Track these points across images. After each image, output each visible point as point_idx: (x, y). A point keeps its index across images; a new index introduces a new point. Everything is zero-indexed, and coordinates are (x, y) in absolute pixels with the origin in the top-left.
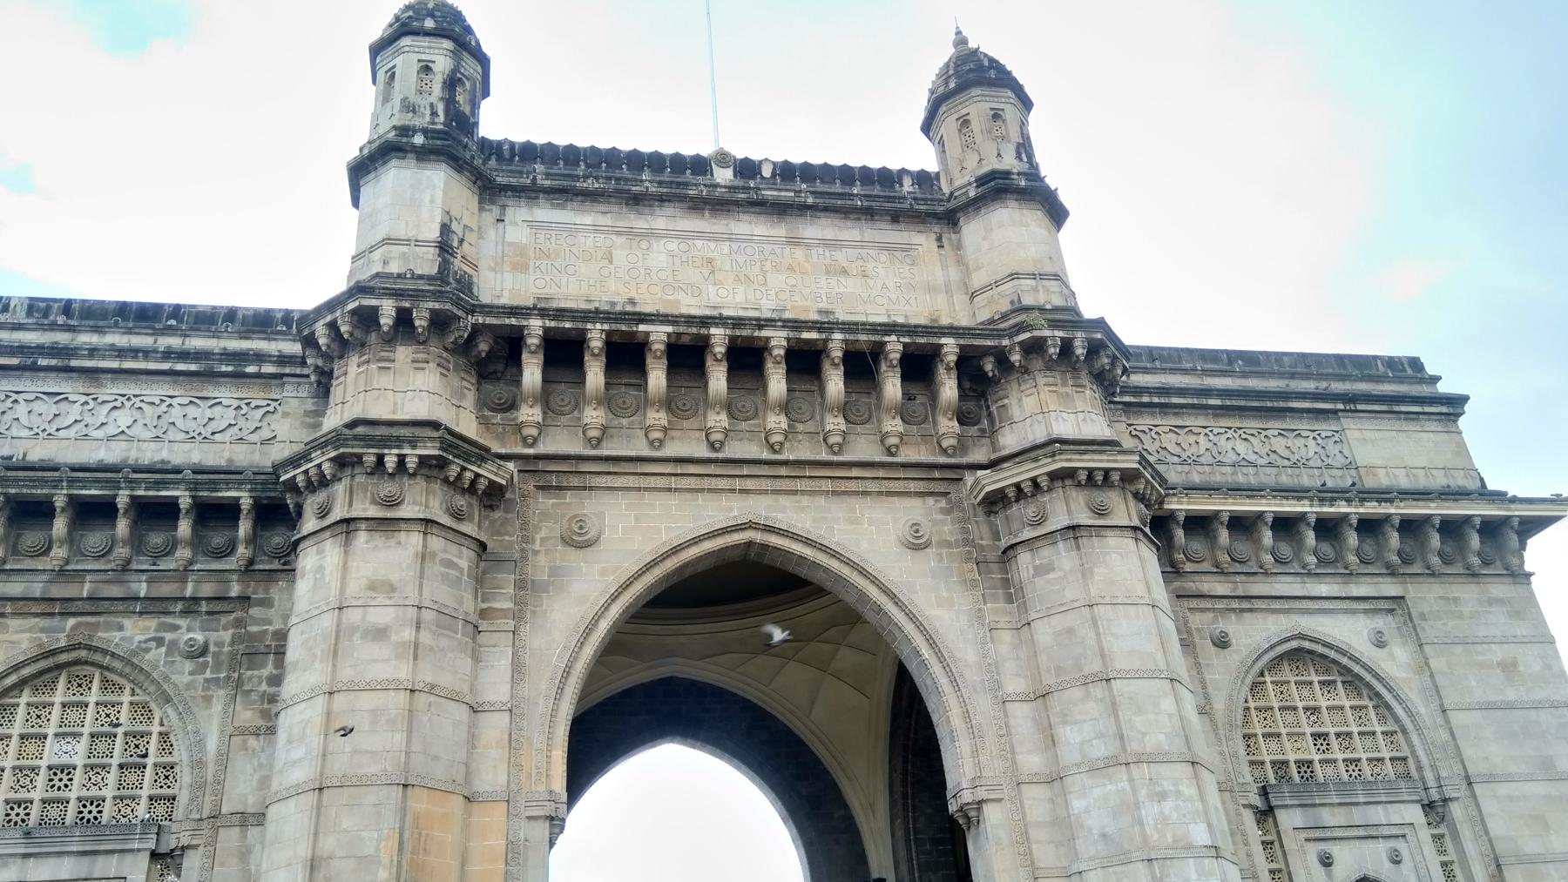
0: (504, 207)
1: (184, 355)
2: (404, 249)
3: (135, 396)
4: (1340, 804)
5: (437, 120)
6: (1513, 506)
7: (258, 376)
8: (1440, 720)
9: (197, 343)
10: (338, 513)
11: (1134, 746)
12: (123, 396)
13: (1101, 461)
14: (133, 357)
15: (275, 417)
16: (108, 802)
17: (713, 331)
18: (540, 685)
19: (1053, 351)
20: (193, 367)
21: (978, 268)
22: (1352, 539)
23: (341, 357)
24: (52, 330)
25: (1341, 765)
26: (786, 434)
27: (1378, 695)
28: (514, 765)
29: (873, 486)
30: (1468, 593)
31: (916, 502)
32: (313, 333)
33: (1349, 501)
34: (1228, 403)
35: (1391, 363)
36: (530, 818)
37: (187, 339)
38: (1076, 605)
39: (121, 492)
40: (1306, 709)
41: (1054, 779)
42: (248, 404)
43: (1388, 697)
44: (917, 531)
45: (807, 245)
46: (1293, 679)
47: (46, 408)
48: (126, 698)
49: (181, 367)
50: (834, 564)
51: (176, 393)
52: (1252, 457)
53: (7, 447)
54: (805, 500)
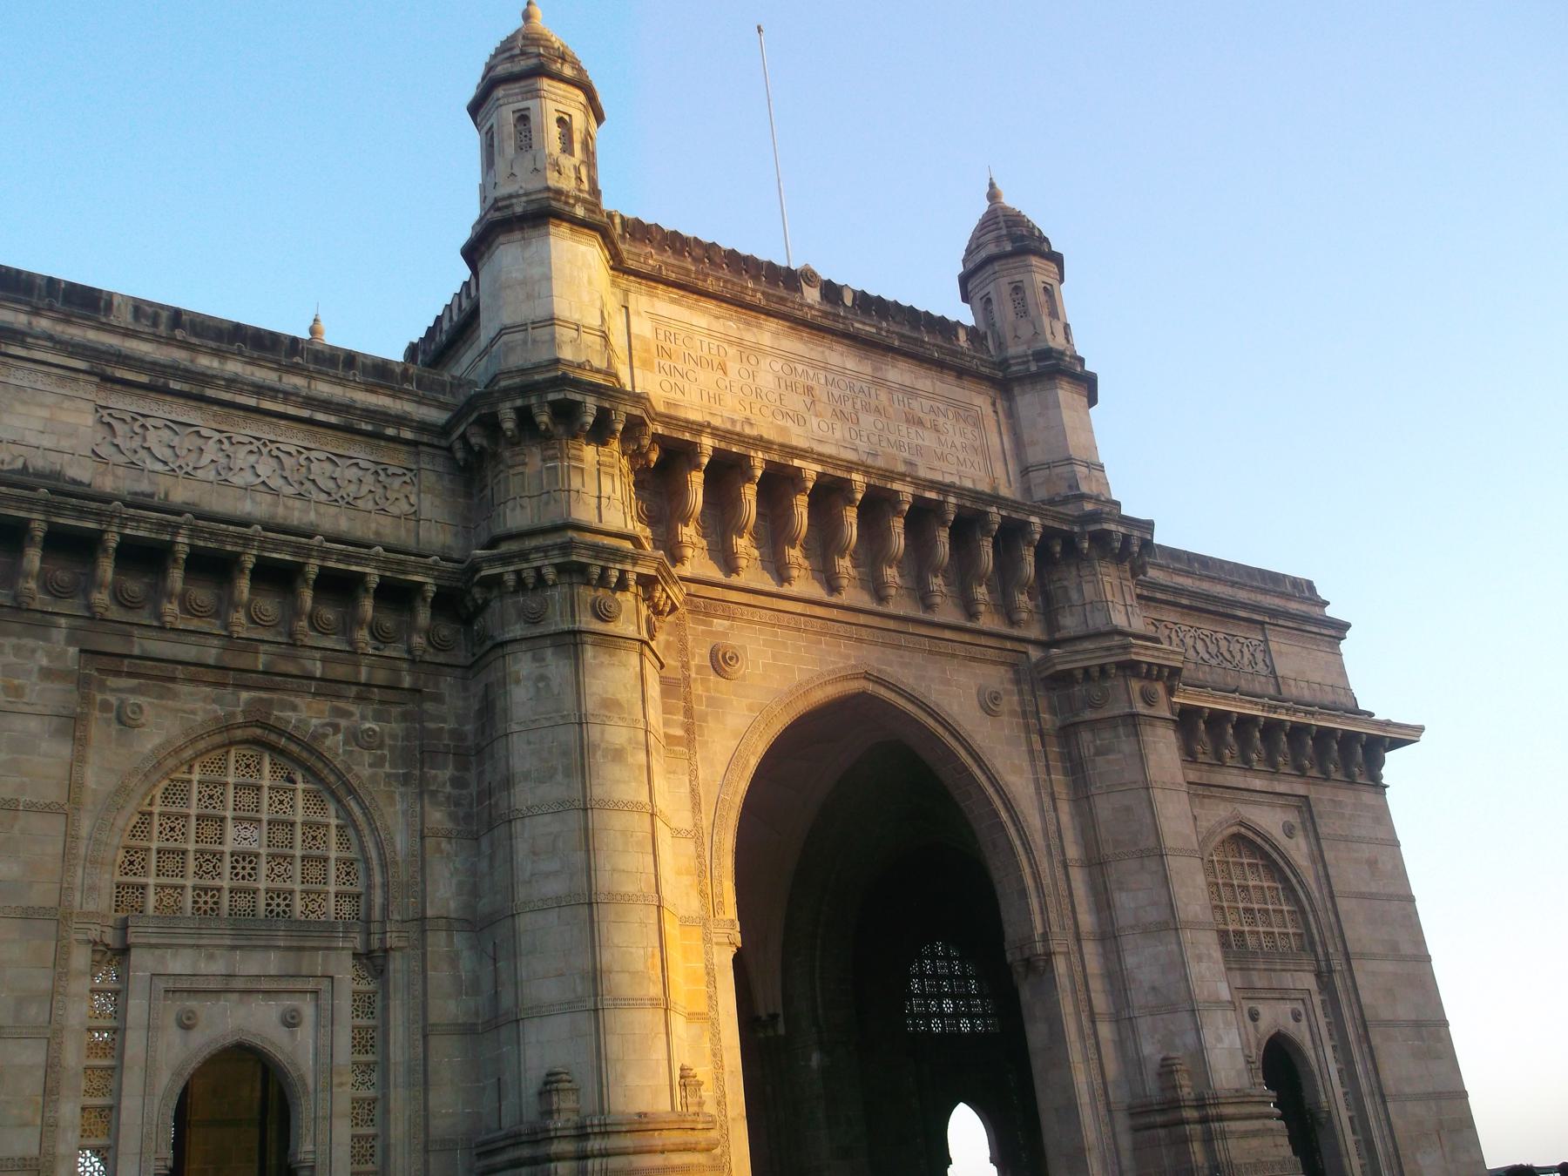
0: (626, 292)
1: (326, 405)
2: (575, 334)
3: (270, 441)
4: (1265, 970)
5: (582, 187)
6: (1388, 728)
7: (395, 440)
8: (1329, 905)
9: (323, 389)
11: (1182, 915)
12: (258, 439)
13: (1158, 657)
14: (271, 397)
15: (409, 488)
16: (298, 896)
17: (855, 476)
19: (1117, 545)
20: (333, 419)
23: (518, 444)
24: (167, 344)
25: (1262, 936)
27: (1285, 880)
28: (702, 893)
29: (960, 650)
32: (494, 415)
33: (1288, 709)
34: (1194, 604)
35: (1296, 582)
36: (717, 944)
37: (313, 382)
38: (1134, 786)
39: (312, 561)
41: (1109, 937)
42: (385, 470)
43: (1294, 881)
44: (996, 698)
45: (889, 388)
46: (1231, 860)
47: (186, 442)
49: (320, 417)
50: (931, 722)
51: (312, 446)
52: (1206, 657)
53: (146, 481)
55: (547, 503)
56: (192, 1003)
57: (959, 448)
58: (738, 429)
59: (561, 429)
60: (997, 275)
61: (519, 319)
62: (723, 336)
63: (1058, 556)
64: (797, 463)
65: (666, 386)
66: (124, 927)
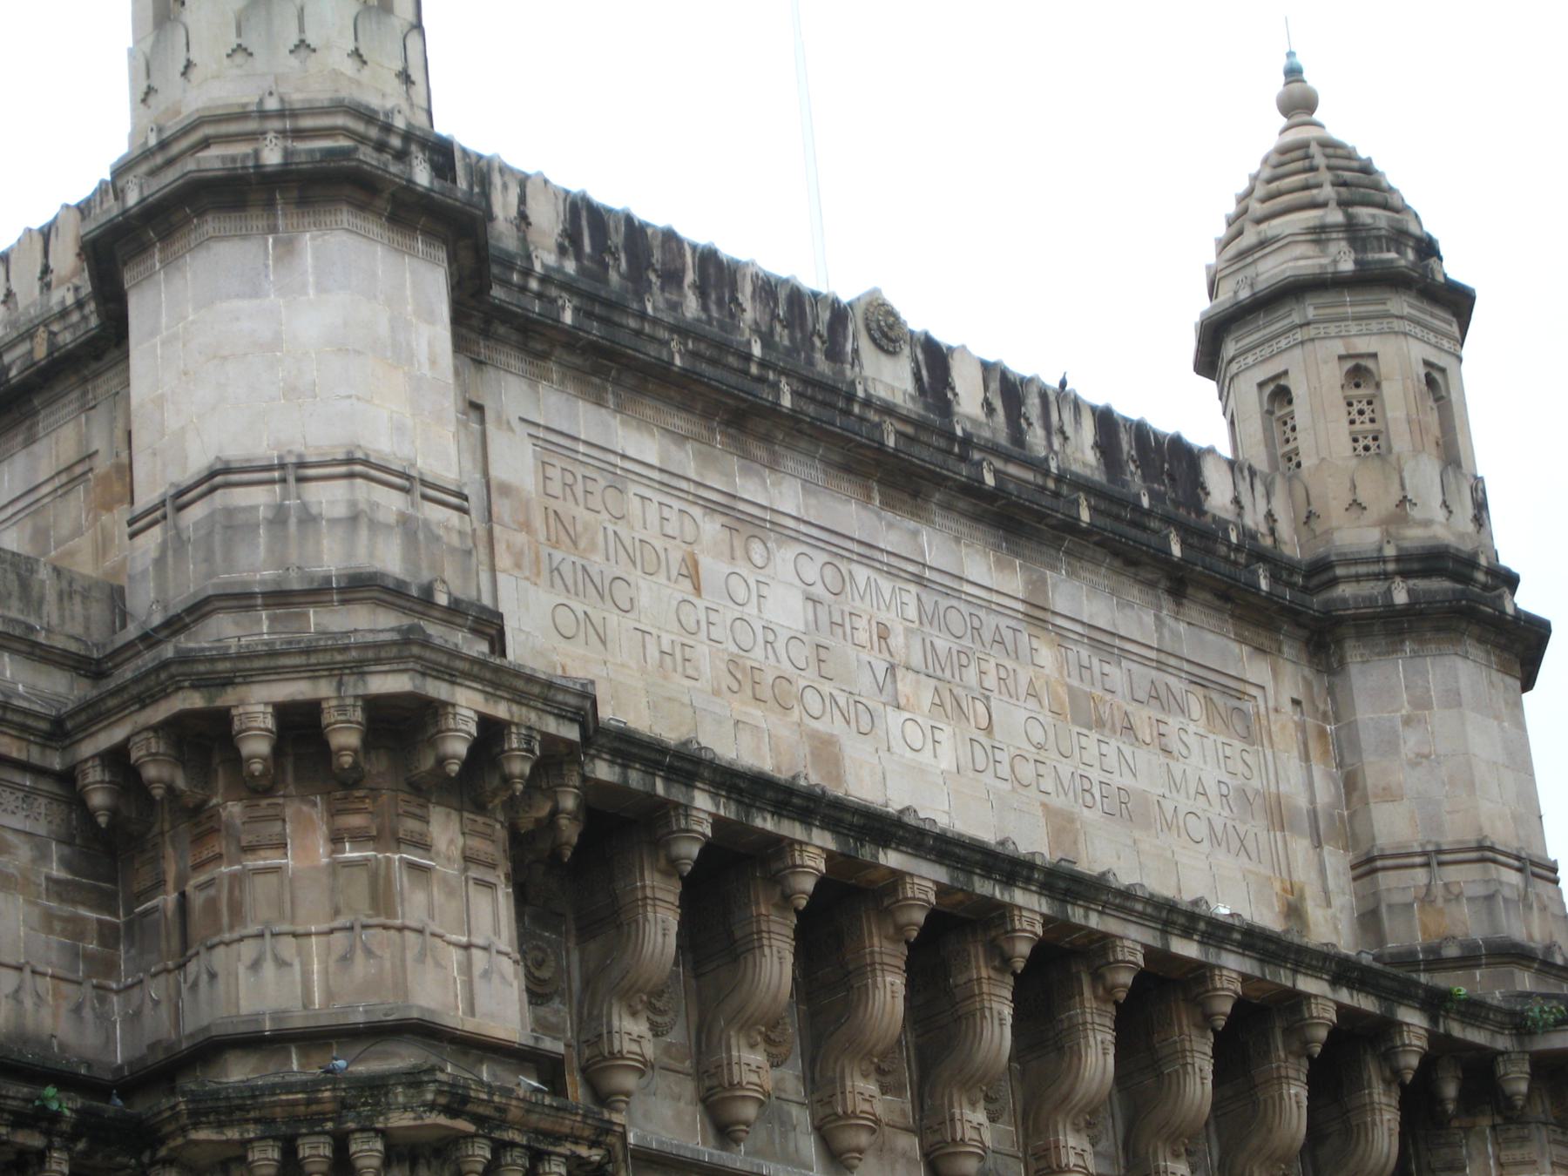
17: (1019, 897)
21: (1390, 795)
23: (268, 792)
55: (346, 959)
57: (1213, 791)
59: (378, 765)
60: (1311, 332)
61: (262, 448)
62: (692, 488)
63: (1451, 1107)
64: (892, 859)
65: (564, 617)
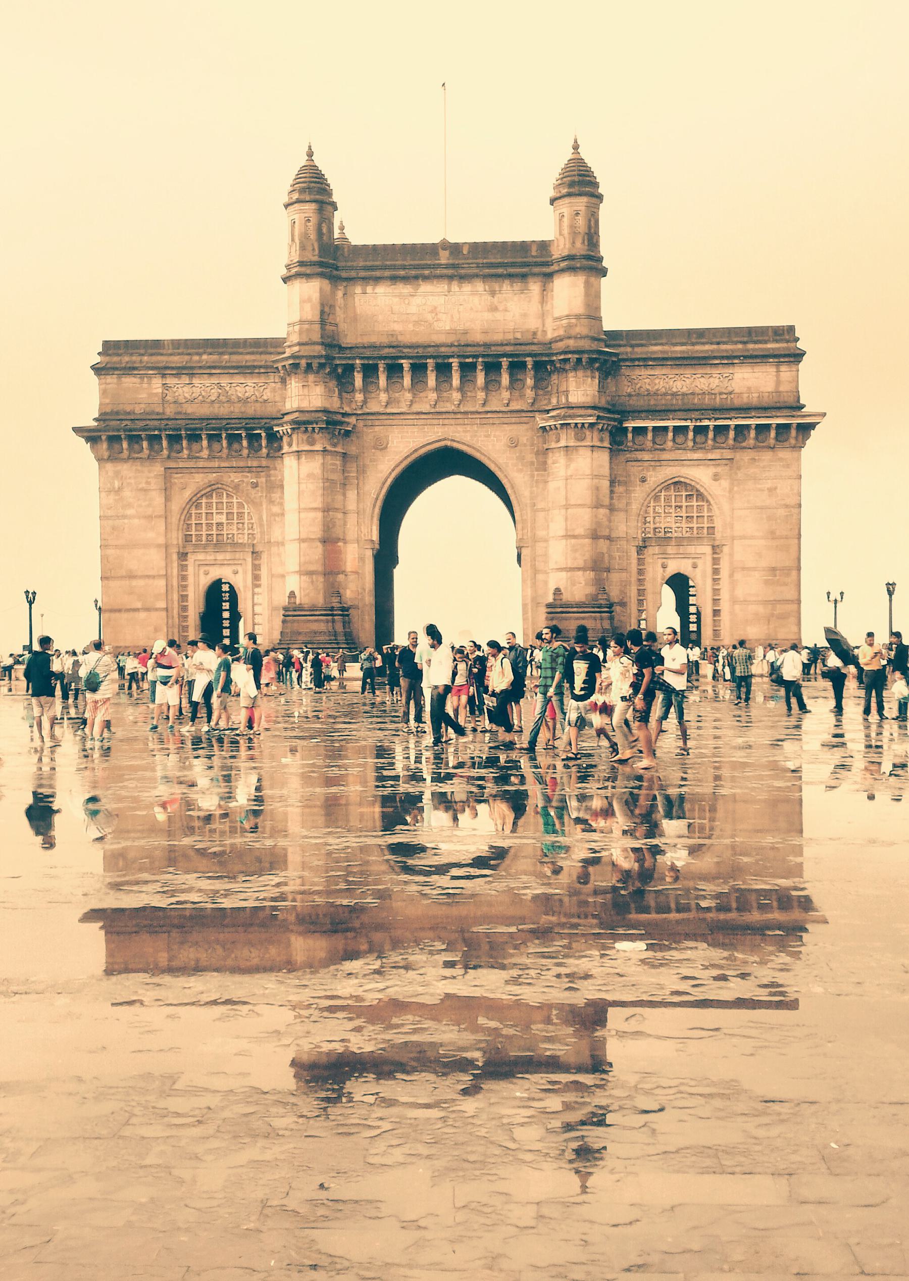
2: (306, 326)
10: (294, 448)
17: (428, 361)
18: (369, 502)
22: (711, 434)
26: (461, 401)
27: (708, 501)
30: (767, 456)
31: (515, 427)
33: (710, 419)
40: (676, 506)
43: (712, 502)
48: (235, 500)
54: (468, 428)
56: (207, 568)
58: (394, 339)
66: (184, 547)
